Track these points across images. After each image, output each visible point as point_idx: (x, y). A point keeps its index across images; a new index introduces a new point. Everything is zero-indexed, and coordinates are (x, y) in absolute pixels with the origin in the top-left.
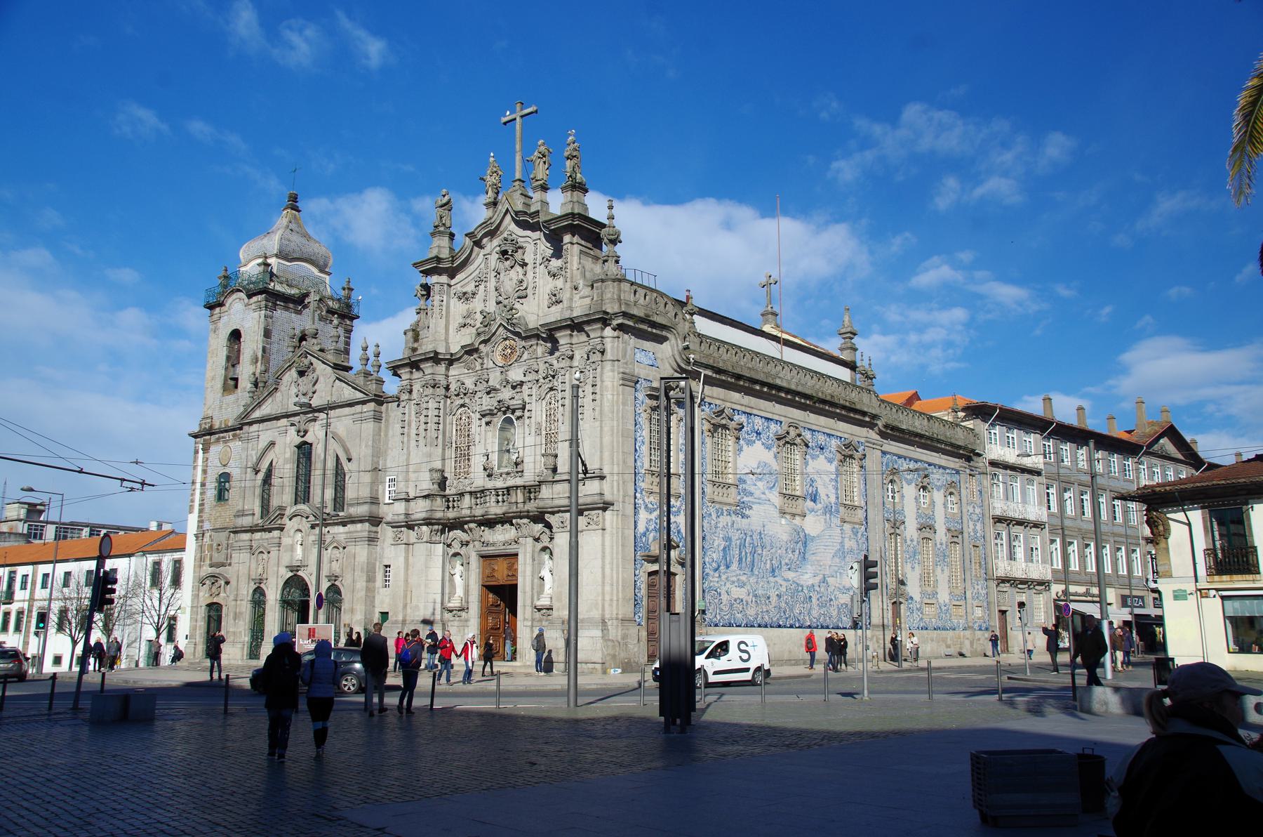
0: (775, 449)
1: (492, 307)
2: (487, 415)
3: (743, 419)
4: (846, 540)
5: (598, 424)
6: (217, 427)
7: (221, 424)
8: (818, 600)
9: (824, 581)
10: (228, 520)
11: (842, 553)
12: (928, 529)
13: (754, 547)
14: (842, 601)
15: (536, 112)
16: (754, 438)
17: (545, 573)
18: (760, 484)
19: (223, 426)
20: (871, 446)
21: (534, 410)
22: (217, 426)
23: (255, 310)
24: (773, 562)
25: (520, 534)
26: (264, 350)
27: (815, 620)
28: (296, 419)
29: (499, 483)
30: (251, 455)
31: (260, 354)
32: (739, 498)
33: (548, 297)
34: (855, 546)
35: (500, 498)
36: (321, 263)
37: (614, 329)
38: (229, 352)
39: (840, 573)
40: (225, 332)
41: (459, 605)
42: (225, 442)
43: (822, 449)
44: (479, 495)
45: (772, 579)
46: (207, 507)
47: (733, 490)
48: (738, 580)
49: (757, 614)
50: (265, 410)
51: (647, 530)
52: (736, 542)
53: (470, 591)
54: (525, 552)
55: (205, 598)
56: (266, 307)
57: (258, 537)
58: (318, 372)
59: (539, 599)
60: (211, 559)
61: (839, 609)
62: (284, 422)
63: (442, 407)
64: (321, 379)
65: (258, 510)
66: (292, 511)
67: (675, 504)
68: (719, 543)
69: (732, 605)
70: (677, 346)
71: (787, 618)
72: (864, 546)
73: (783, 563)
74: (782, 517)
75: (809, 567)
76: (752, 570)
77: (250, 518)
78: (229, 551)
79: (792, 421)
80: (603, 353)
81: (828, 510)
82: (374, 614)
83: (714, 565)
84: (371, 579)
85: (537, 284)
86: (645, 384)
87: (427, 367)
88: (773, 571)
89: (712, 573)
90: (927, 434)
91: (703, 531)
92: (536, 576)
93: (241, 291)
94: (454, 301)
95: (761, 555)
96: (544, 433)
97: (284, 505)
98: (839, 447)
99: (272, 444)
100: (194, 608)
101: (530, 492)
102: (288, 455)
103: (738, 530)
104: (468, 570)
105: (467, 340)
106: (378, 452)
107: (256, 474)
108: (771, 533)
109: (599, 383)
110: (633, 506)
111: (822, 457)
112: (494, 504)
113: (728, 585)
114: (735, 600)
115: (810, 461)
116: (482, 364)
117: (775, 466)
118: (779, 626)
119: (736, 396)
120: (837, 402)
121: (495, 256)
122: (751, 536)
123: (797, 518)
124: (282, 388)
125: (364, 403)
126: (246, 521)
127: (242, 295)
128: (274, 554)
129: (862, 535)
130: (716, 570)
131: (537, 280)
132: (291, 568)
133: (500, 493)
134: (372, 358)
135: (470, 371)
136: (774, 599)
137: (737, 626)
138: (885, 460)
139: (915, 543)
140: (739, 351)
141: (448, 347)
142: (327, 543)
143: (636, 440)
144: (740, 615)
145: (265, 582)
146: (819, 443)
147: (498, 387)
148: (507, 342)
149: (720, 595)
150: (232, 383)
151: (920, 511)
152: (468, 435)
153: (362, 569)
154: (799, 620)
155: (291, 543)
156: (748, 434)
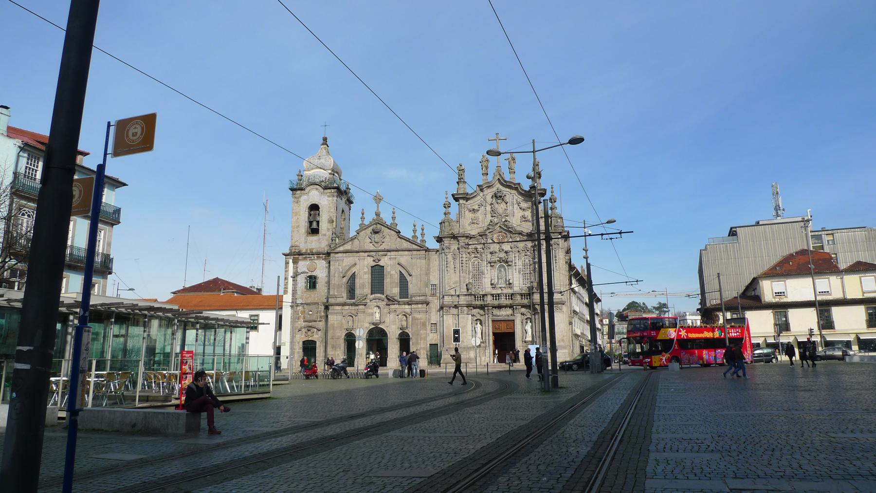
2: (491, 264)
6: (303, 252)
19: (309, 252)
23: (329, 196)
25: (515, 312)
35: (507, 297)
42: (311, 260)
46: (299, 293)
50: (348, 247)
55: (301, 338)
57: (347, 308)
65: (345, 295)
77: (341, 299)
78: (319, 314)
87: (463, 241)
100: (292, 343)
102: (366, 270)
107: (343, 277)
126: (339, 300)
133: (507, 295)
150: (314, 231)
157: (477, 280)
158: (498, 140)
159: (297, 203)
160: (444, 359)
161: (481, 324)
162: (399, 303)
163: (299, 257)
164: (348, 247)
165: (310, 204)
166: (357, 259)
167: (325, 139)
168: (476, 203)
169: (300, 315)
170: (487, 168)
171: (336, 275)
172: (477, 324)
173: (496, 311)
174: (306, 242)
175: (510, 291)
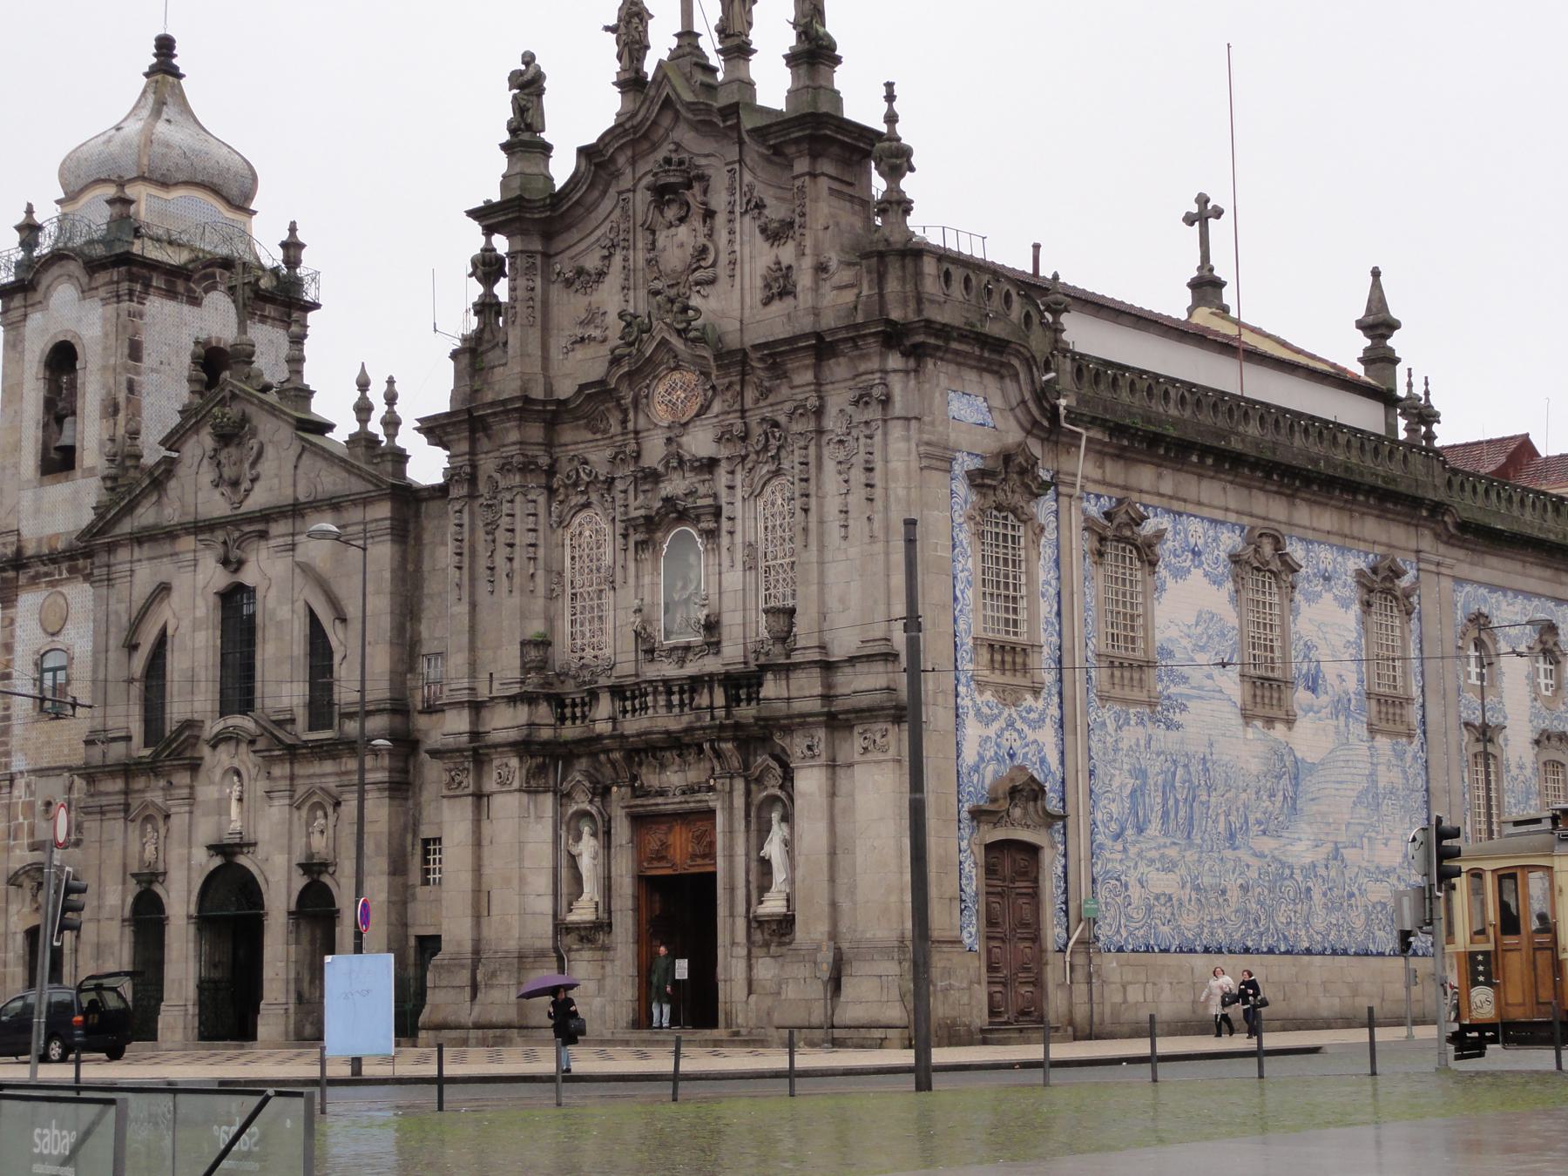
0: (1229, 585)
1: (640, 303)
3: (1165, 522)
4: (1382, 768)
5: (879, 547)
7: (40, 541)
8: (1325, 895)
9: (1336, 854)
10: (66, 751)
11: (1372, 797)
12: (1554, 742)
13: (1193, 789)
14: (1375, 898)
16: (1188, 563)
17: (774, 849)
18: (1201, 658)
19: (46, 550)
20: (1433, 568)
21: (739, 514)
22: (30, 550)
23: (105, 302)
24: (1232, 818)
26: (131, 387)
27: (1319, 938)
28: (220, 535)
29: (669, 669)
30: (117, 613)
31: (122, 397)
32: (1159, 688)
33: (759, 283)
34: (1399, 781)
35: (675, 699)
36: (234, 191)
37: (906, 354)
38: (50, 390)
39: (1370, 838)
40: (37, 347)
41: (593, 917)
42: (52, 584)
43: (1327, 579)
44: (628, 694)
45: (1229, 854)
47: (1153, 673)
48: (1163, 856)
49: (1201, 927)
50: (146, 515)
51: (982, 758)
52: (1155, 779)
53: (613, 888)
54: (730, 809)
56: (131, 293)
58: (262, 437)
59: (761, 902)
60: (32, 833)
61: (1368, 914)
62: (187, 543)
63: (542, 511)
64: (270, 451)
65: (137, 728)
66: (217, 729)
67: (1034, 705)
68: (1121, 781)
69: (1150, 908)
70: (1033, 381)
71: (1261, 934)
72: (1420, 782)
73: (1251, 820)
74: (1247, 724)
75: (1303, 825)
76: (1189, 836)
79: (1267, 524)
80: (886, 402)
81: (1341, 707)
82: (406, 937)
83: (1114, 826)
84: (398, 867)
85: (738, 254)
86: (973, 464)
88: (1232, 836)
89: (1109, 843)
90: (1552, 537)
91: (1091, 758)
92: (753, 855)
93: (74, 259)
94: (556, 291)
95: (1207, 804)
96: (762, 564)
97: (197, 717)
98: (1360, 573)
99: (163, 589)
101: (739, 687)
102: (201, 612)
103: (1158, 754)
104: (607, 846)
105: (596, 371)
106: (408, 609)
108: (1226, 758)
109: (878, 466)
110: (952, 713)
111: (1327, 597)
112: (662, 711)
113: (1142, 868)
114: (1157, 898)
115: (1304, 606)
116: (624, 422)
117: (1231, 617)
118: (1247, 950)
119: (1144, 476)
120: (1358, 479)
121: (642, 198)
122: (1186, 766)
123: (1280, 727)
124: (183, 471)
125: (365, 501)
126: (117, 751)
127: (74, 267)
128: (178, 822)
129: (1415, 758)
130: (1117, 837)
131: (737, 247)
132: (217, 849)
133: (676, 689)
134: (380, 409)
135: (599, 436)
136: (1234, 895)
137: (1161, 951)
138: (1460, 597)
139: (1528, 772)
140: (1153, 383)
141: (549, 388)
142: (297, 797)
143: (955, 577)
144: (1166, 929)
145: (161, 879)
146: (1322, 566)
147: (661, 468)
148: (676, 376)
149: (1127, 889)
151: (1538, 704)
152: (598, 570)
153: (378, 846)
154: (1285, 938)
155: (216, 795)
156: (1176, 556)
159: (14, 346)
160: (436, 1006)
161: (594, 835)
162: (293, 752)
163: (17, 578)
164: (146, 515)
165: (50, 346)
166: (166, 570)
167: (165, 46)
168: (593, 238)
169: (21, 819)
171: (112, 643)
174: (38, 511)
175: (711, 665)
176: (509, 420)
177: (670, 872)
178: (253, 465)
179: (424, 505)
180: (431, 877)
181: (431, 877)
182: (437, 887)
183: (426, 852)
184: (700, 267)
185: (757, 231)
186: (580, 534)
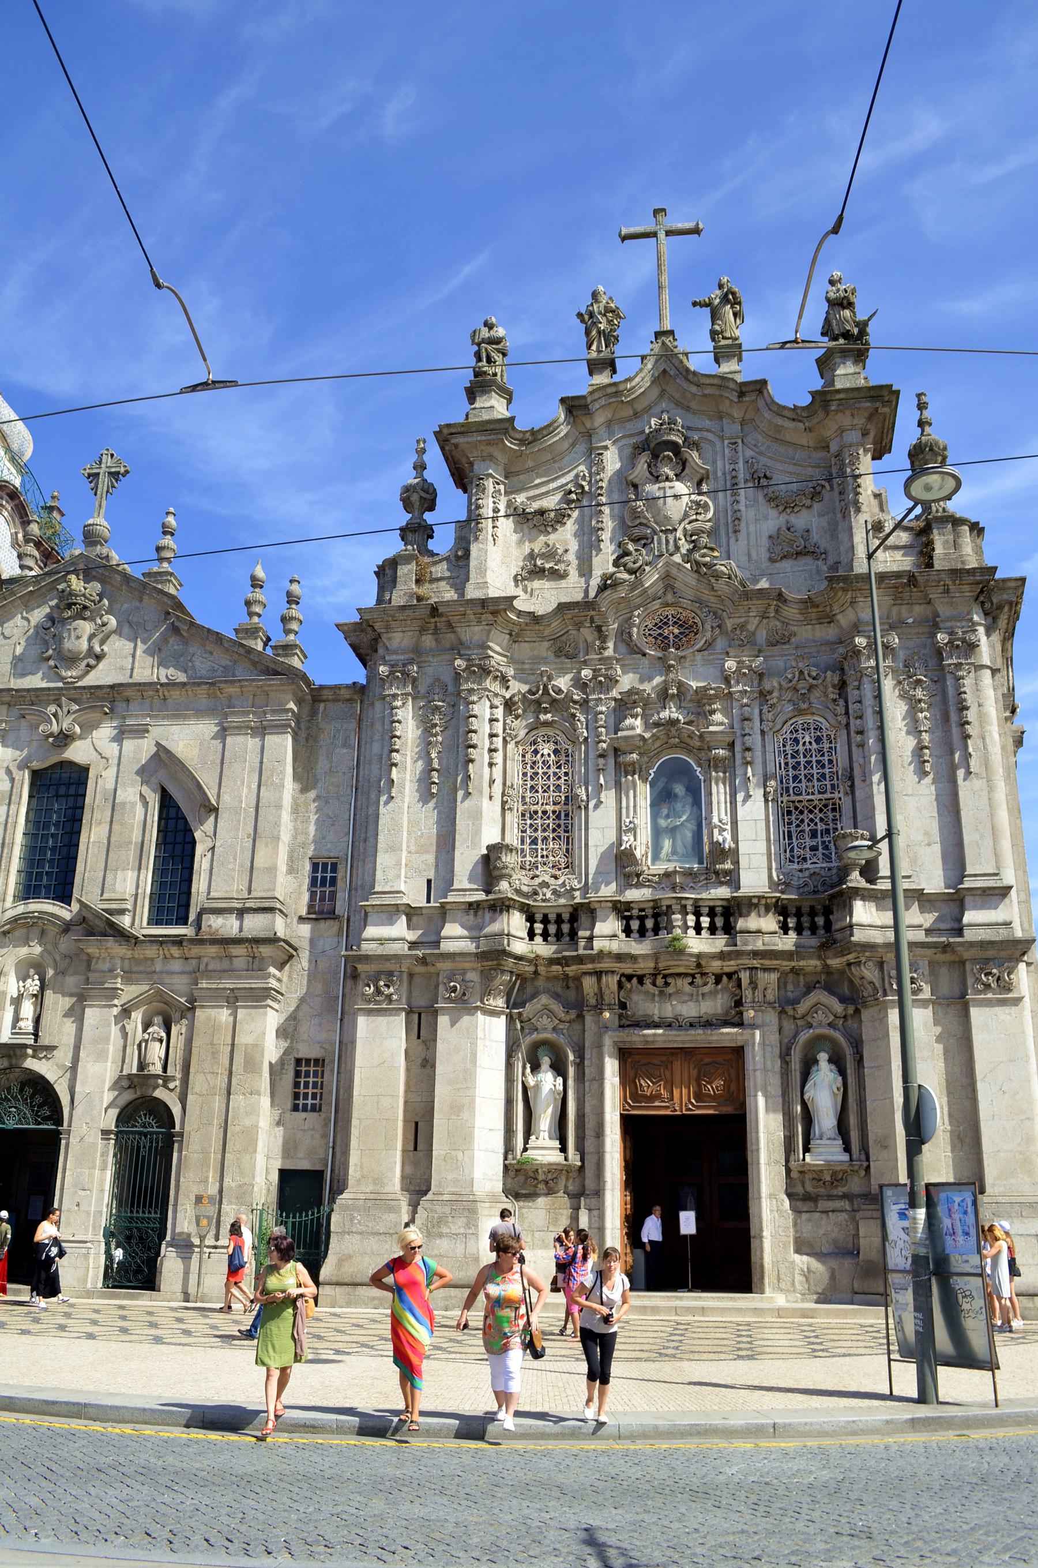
15: (696, 231)
33: (765, 542)
35: (705, 921)
37: (986, 614)
85: (744, 514)
112: (691, 932)
131: (743, 509)
133: (705, 910)
148: (670, 611)
157: (545, 839)
158: (662, 235)
161: (559, 1069)
170: (610, 338)
172: (536, 1068)
173: (643, 1004)
176: (479, 622)
177: (668, 1112)
178: (102, 642)
179: (322, 706)
180: (301, 1102)
181: (301, 1102)
182: (312, 1116)
183: (298, 1074)
184: (697, 520)
185: (761, 499)
186: (536, 752)
